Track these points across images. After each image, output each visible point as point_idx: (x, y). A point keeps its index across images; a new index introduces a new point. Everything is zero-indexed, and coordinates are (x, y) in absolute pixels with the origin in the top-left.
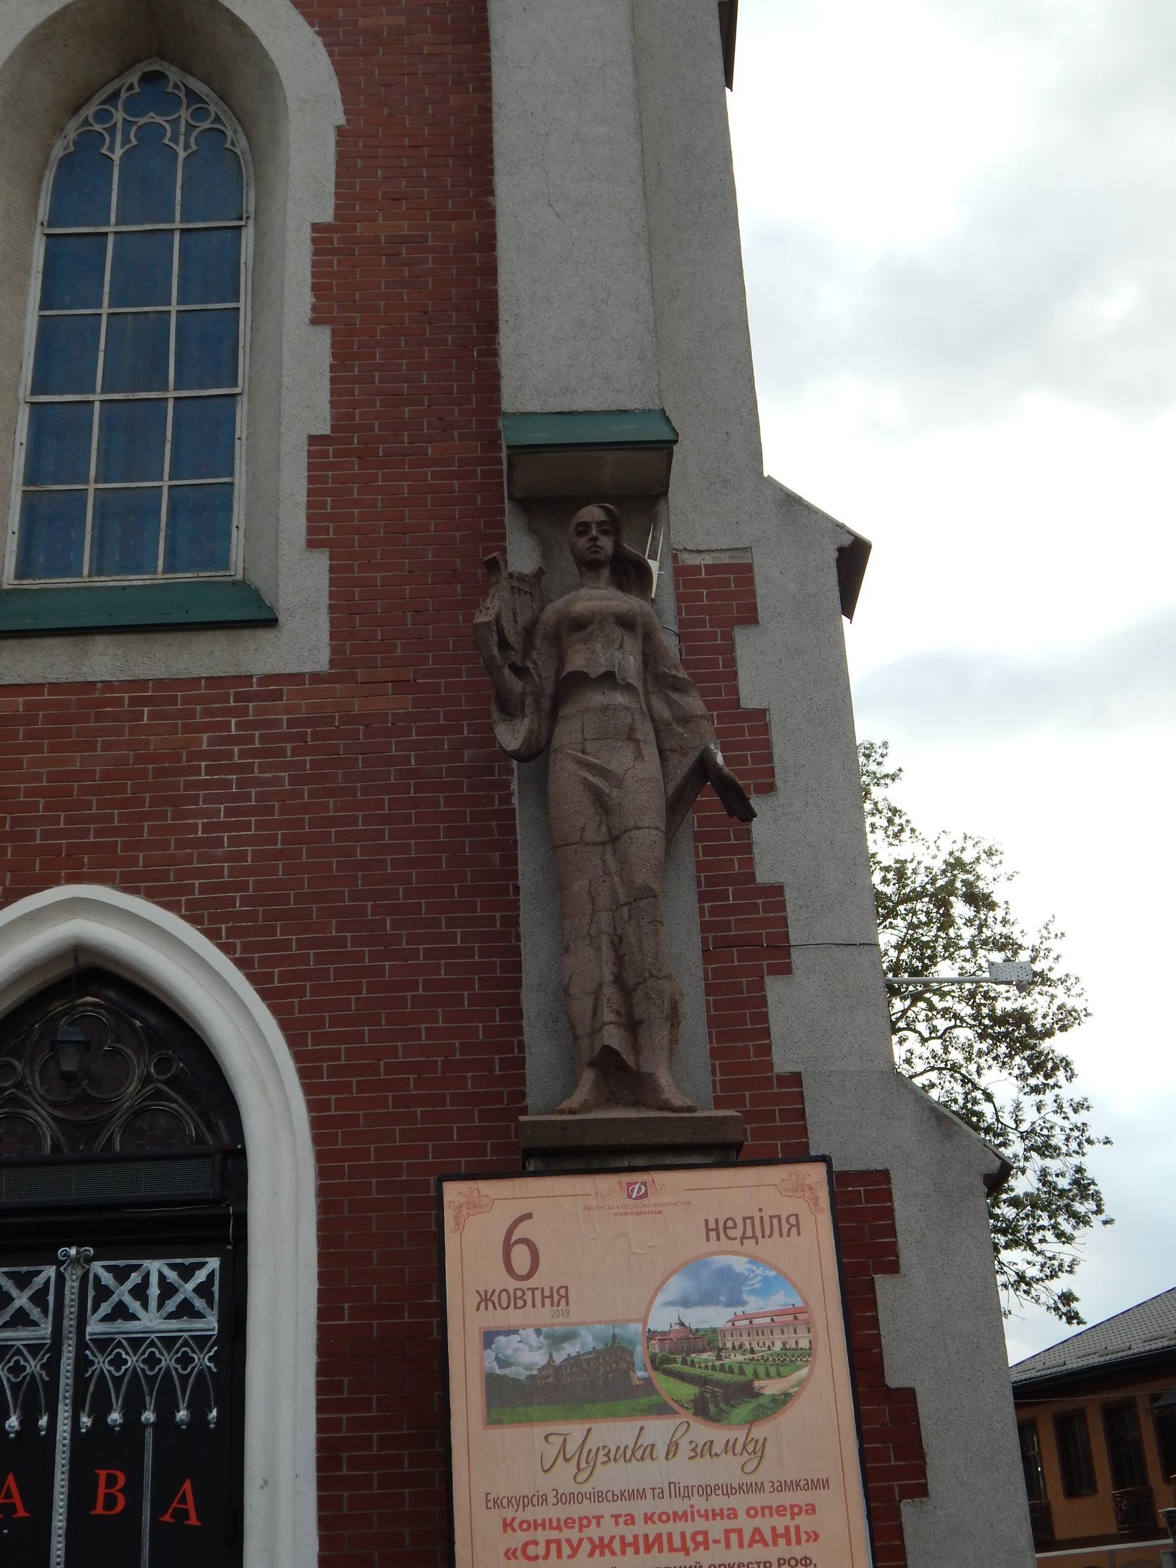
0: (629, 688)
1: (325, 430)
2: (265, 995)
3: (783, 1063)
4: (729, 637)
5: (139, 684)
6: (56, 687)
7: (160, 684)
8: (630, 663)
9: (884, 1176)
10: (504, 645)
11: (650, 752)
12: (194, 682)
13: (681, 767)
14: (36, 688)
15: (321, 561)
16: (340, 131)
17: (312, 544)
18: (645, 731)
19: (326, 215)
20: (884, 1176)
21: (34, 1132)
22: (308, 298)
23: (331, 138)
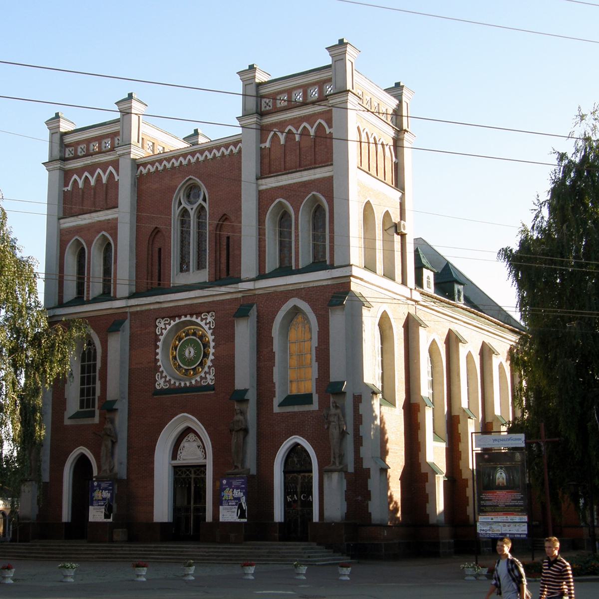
0: (335, 422)
1: (317, 377)
2: (313, 448)
3: (361, 456)
4: (359, 405)
5: (300, 412)
6: (292, 412)
7: (302, 412)
8: (336, 419)
9: (370, 469)
10: (325, 417)
11: (338, 429)
12: (304, 411)
13: (341, 430)
14: (289, 412)
15: (317, 395)
16: (318, 331)
17: (316, 393)
18: (337, 427)
19: (317, 346)
20: (370, 469)
21: (295, 461)
22: (315, 358)
23: (317, 333)
